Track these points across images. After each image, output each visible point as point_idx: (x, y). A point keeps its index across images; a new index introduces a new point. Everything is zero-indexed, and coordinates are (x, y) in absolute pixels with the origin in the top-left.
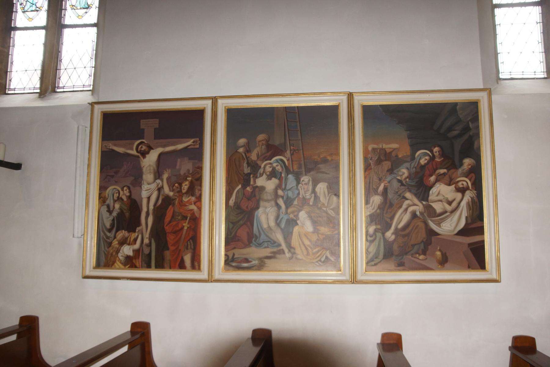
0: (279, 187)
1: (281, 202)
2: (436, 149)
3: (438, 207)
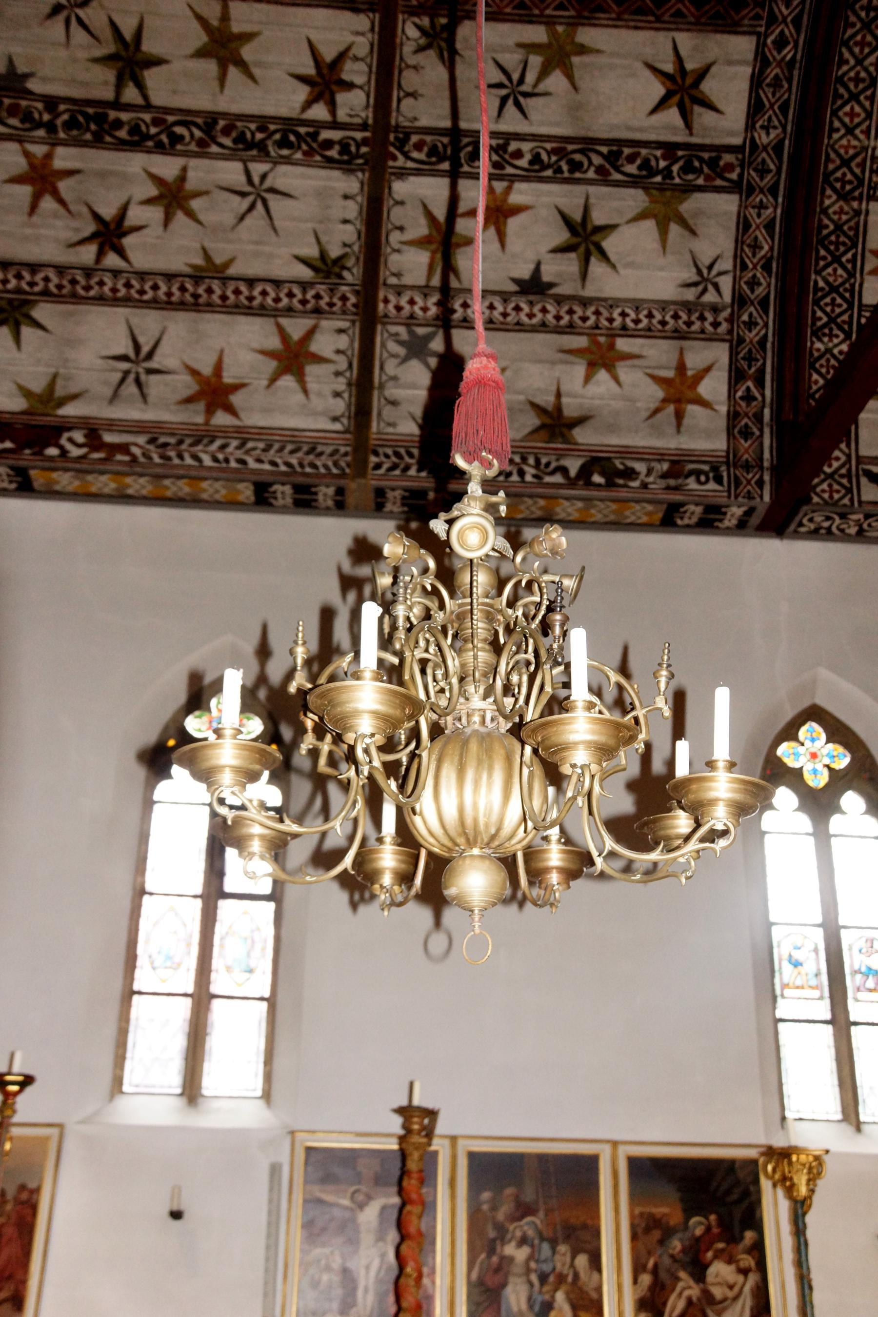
0: (530, 1257)
1: (534, 1278)
2: (713, 1217)
3: (718, 1292)
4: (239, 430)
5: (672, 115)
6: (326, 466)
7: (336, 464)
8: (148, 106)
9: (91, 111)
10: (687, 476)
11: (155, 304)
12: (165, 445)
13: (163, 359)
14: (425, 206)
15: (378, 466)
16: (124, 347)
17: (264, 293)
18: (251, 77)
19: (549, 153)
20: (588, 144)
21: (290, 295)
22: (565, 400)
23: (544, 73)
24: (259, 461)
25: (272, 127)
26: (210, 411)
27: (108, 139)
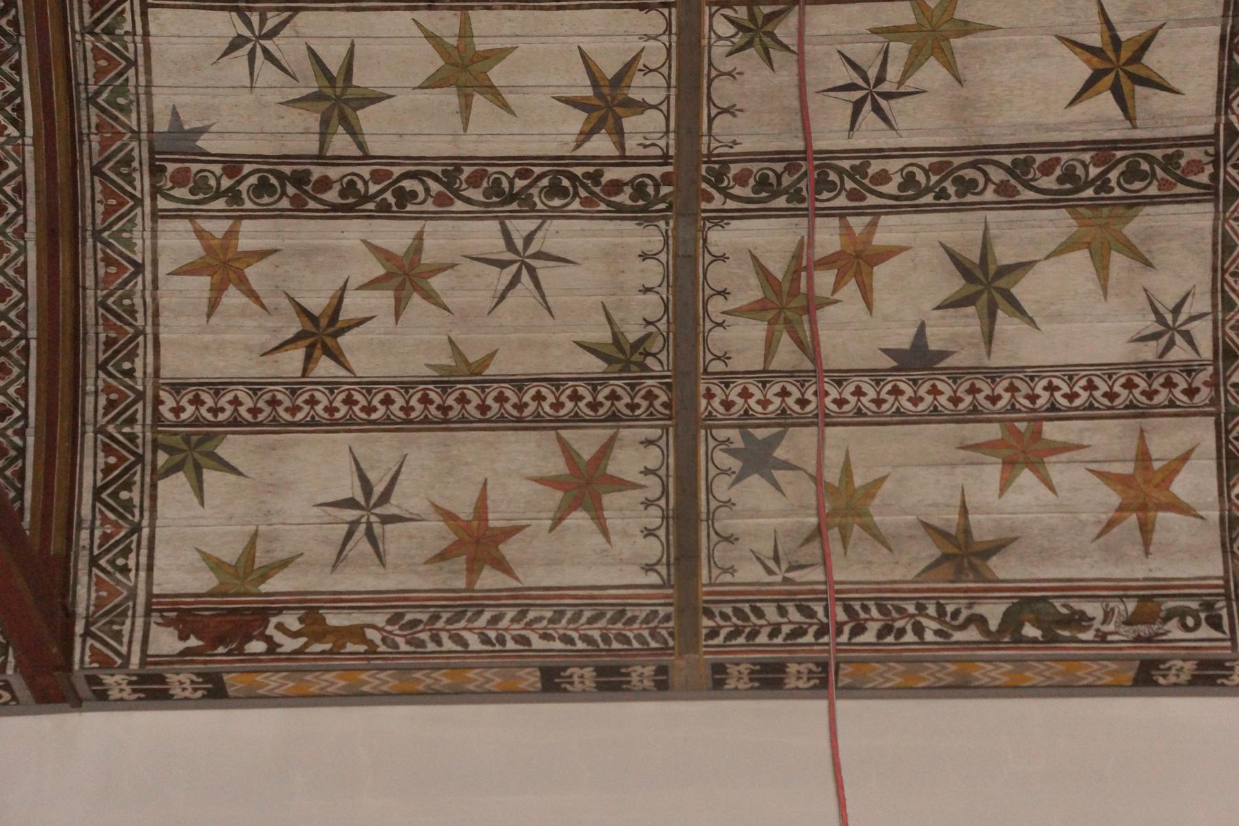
4: (515, 593)
5: (1104, 103)
6: (640, 638)
7: (653, 633)
8: (366, 157)
9: (287, 170)
10: (1166, 619)
11: (388, 424)
12: (415, 623)
13: (405, 499)
14: (755, 259)
15: (713, 633)
16: (349, 487)
17: (539, 397)
18: (505, 106)
19: (926, 172)
20: (982, 154)
21: (575, 397)
22: (973, 518)
23: (911, 67)
24: (545, 637)
25: (537, 170)
26: (473, 571)
27: (312, 204)
